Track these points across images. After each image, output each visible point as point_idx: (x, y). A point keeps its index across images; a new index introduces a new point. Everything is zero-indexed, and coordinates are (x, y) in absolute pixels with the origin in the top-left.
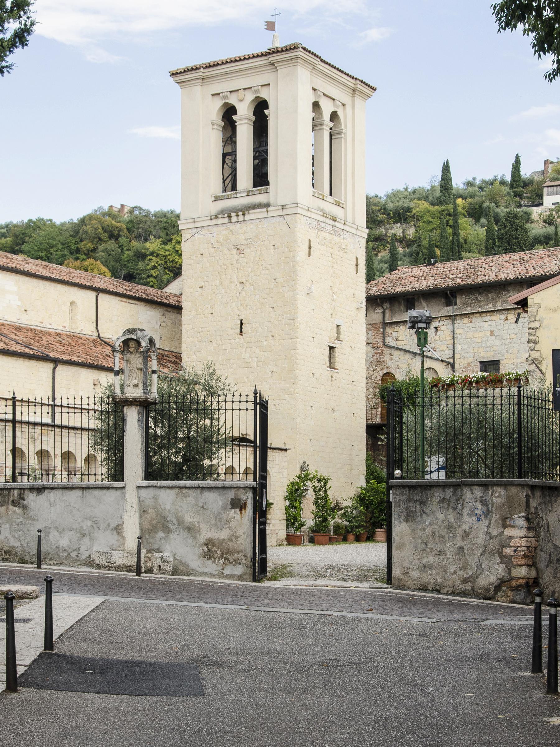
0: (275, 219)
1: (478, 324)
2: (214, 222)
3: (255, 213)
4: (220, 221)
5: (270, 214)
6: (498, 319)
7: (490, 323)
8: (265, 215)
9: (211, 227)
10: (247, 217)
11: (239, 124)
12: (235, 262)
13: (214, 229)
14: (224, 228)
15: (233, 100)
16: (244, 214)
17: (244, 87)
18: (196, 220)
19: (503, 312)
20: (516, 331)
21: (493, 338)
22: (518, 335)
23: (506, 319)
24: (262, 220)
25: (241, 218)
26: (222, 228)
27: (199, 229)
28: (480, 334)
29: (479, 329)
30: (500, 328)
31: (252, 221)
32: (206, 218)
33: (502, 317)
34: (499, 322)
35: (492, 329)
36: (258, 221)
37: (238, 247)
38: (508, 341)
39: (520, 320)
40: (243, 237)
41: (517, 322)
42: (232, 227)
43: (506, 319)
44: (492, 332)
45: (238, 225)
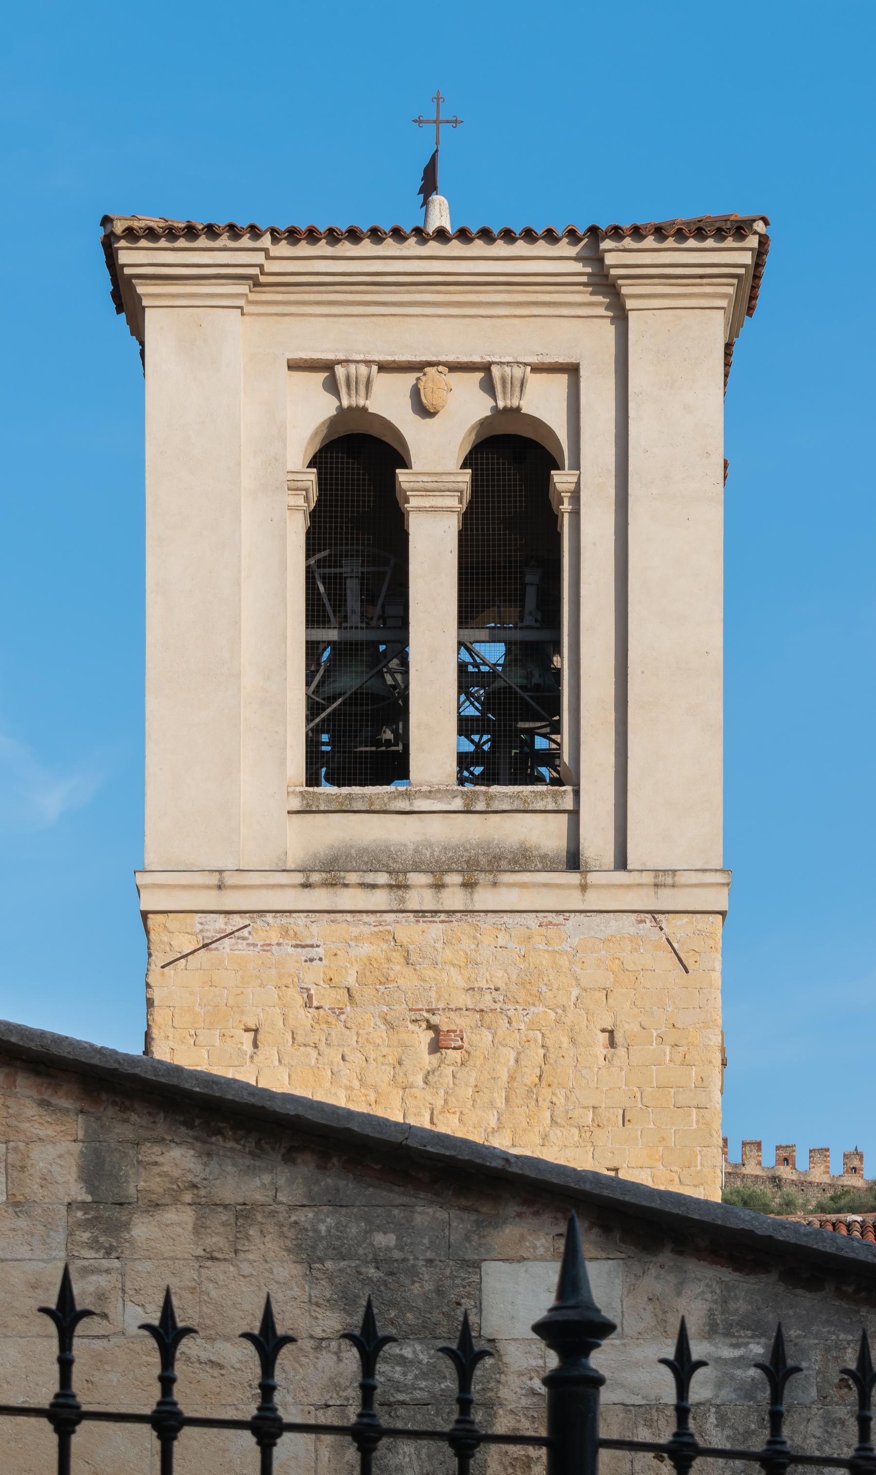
0: (614, 924)
2: (320, 899)
3: (523, 885)
4: (348, 899)
5: (593, 900)
8: (575, 901)
9: (301, 919)
10: (484, 898)
11: (419, 509)
12: (419, 1080)
13: (317, 930)
14: (365, 929)
15: (388, 401)
16: (469, 885)
17: (451, 358)
18: (230, 879)
24: (551, 917)
25: (454, 898)
26: (355, 931)
27: (238, 921)
31: (506, 918)
32: (283, 878)
36: (531, 921)
37: (435, 1020)
40: (458, 979)
42: (408, 931)
45: (436, 930)
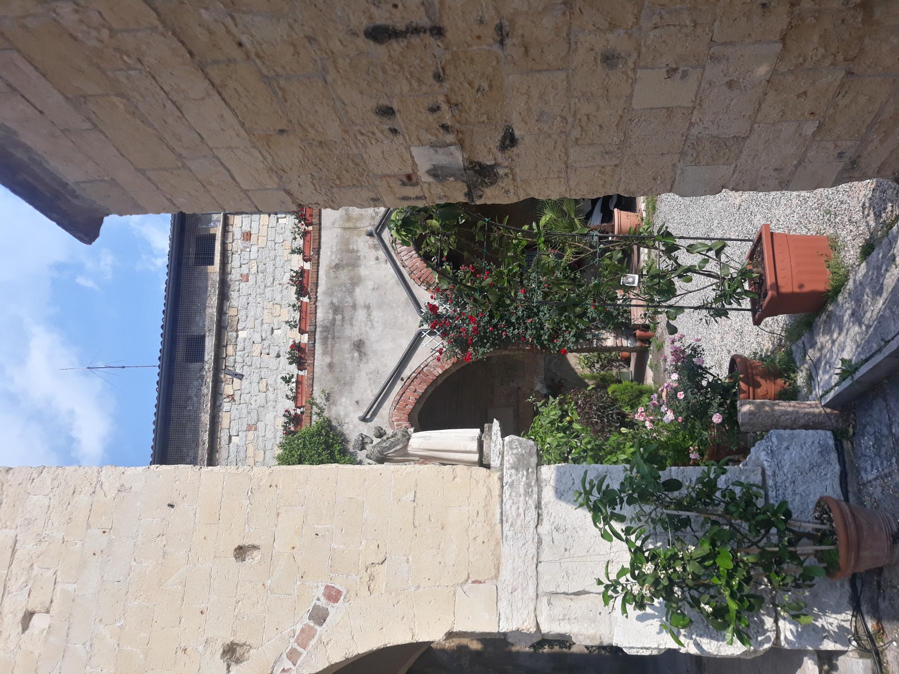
1: (232, 455)
6: (229, 414)
7: (233, 433)
19: (218, 403)
20: (255, 378)
21: (260, 425)
22: (263, 375)
23: (232, 398)
28: (250, 453)
29: (242, 455)
30: (245, 411)
33: (226, 406)
34: (234, 413)
35: (245, 427)
38: (271, 396)
39: (238, 371)
41: (241, 377)
43: (232, 398)
44: (250, 428)
